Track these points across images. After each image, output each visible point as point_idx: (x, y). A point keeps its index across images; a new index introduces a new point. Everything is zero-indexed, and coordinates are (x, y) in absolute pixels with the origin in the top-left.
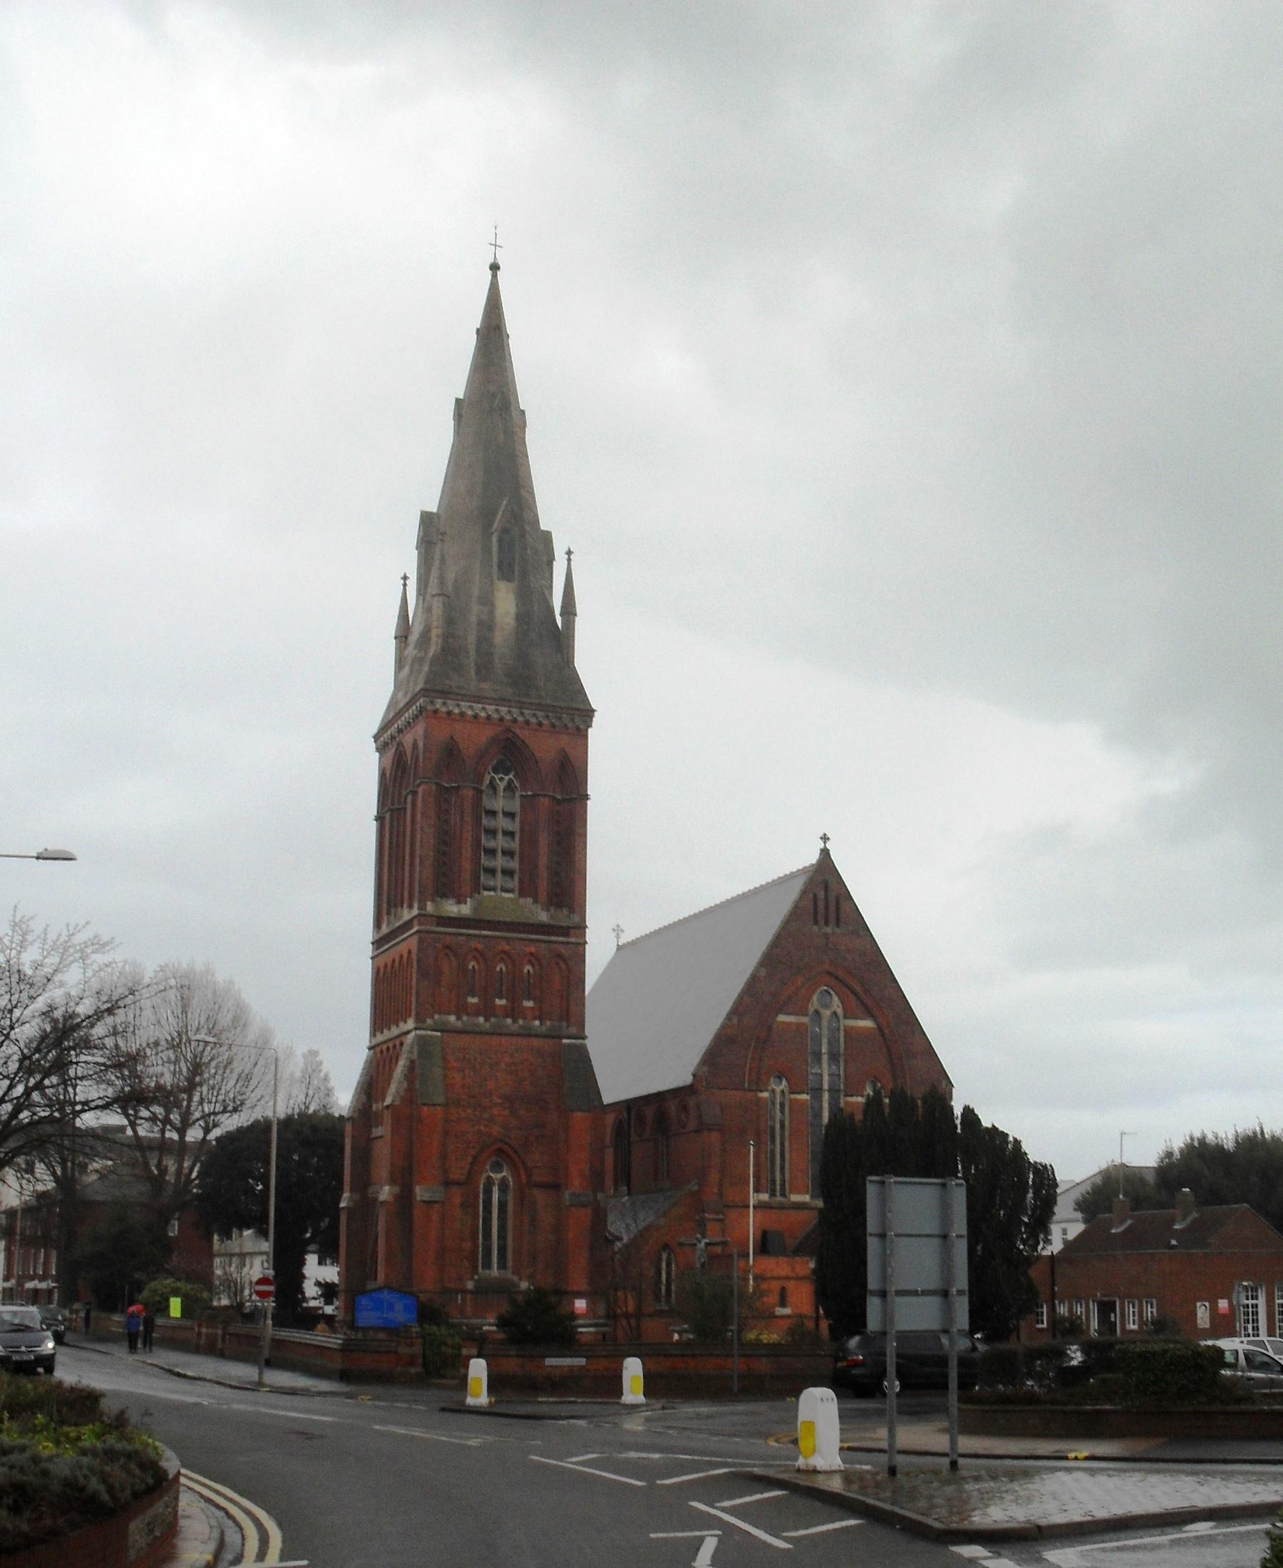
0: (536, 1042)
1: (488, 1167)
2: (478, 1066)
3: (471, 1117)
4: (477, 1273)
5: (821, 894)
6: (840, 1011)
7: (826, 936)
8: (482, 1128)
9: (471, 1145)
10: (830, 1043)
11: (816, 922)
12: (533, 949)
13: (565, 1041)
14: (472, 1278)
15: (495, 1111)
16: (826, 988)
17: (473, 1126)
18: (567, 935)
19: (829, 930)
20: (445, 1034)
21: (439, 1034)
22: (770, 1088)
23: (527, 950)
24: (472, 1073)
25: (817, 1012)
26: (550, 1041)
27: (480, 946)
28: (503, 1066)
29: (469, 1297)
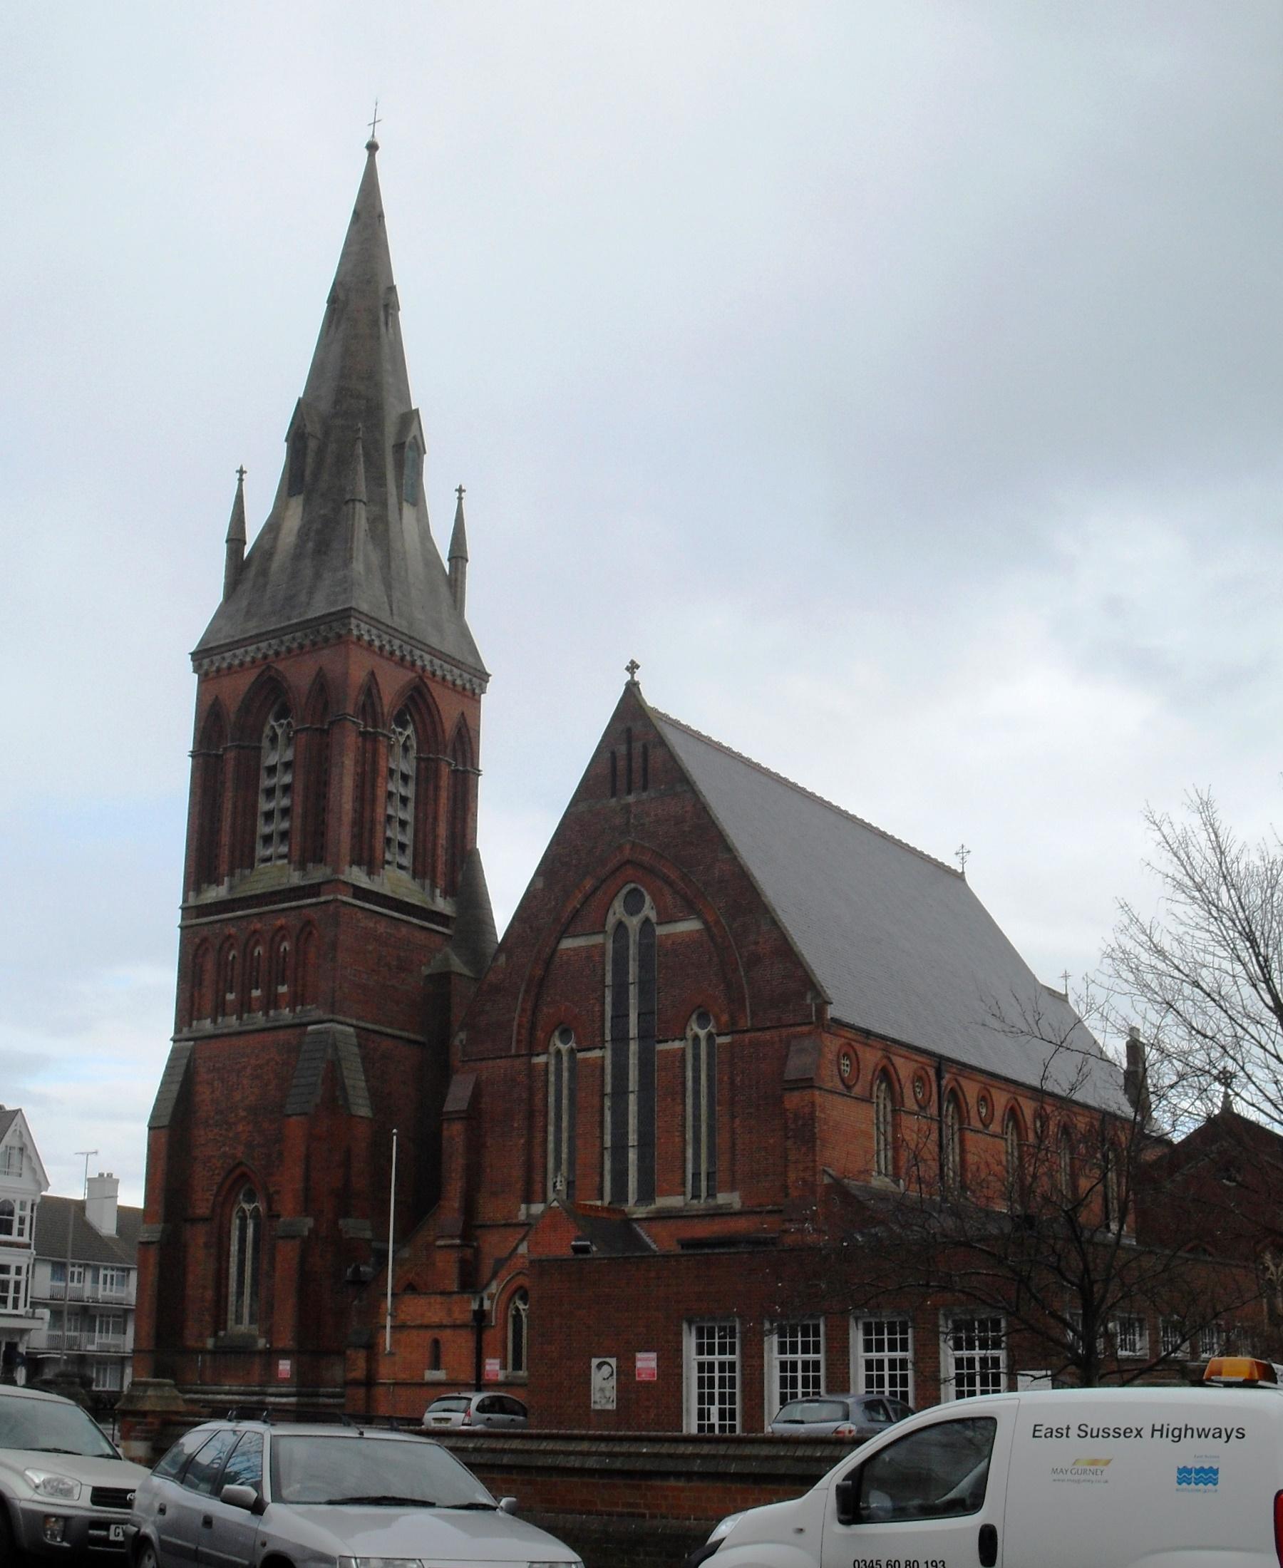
0: (281, 1035)
1: (241, 1197)
2: (226, 1076)
3: (217, 1137)
4: (225, 1329)
5: (623, 749)
6: (653, 916)
7: (627, 809)
8: (227, 1149)
9: (216, 1172)
10: (641, 967)
11: (613, 795)
12: (281, 921)
13: (310, 1028)
14: (215, 1335)
15: (240, 1128)
16: (633, 885)
17: (221, 1147)
18: (318, 895)
19: (631, 799)
20: (199, 1042)
21: (192, 1043)
22: (552, 1049)
23: (279, 923)
24: (220, 1085)
25: (620, 925)
26: (298, 1031)
27: (233, 931)
28: (249, 1071)
29: (208, 1358)
